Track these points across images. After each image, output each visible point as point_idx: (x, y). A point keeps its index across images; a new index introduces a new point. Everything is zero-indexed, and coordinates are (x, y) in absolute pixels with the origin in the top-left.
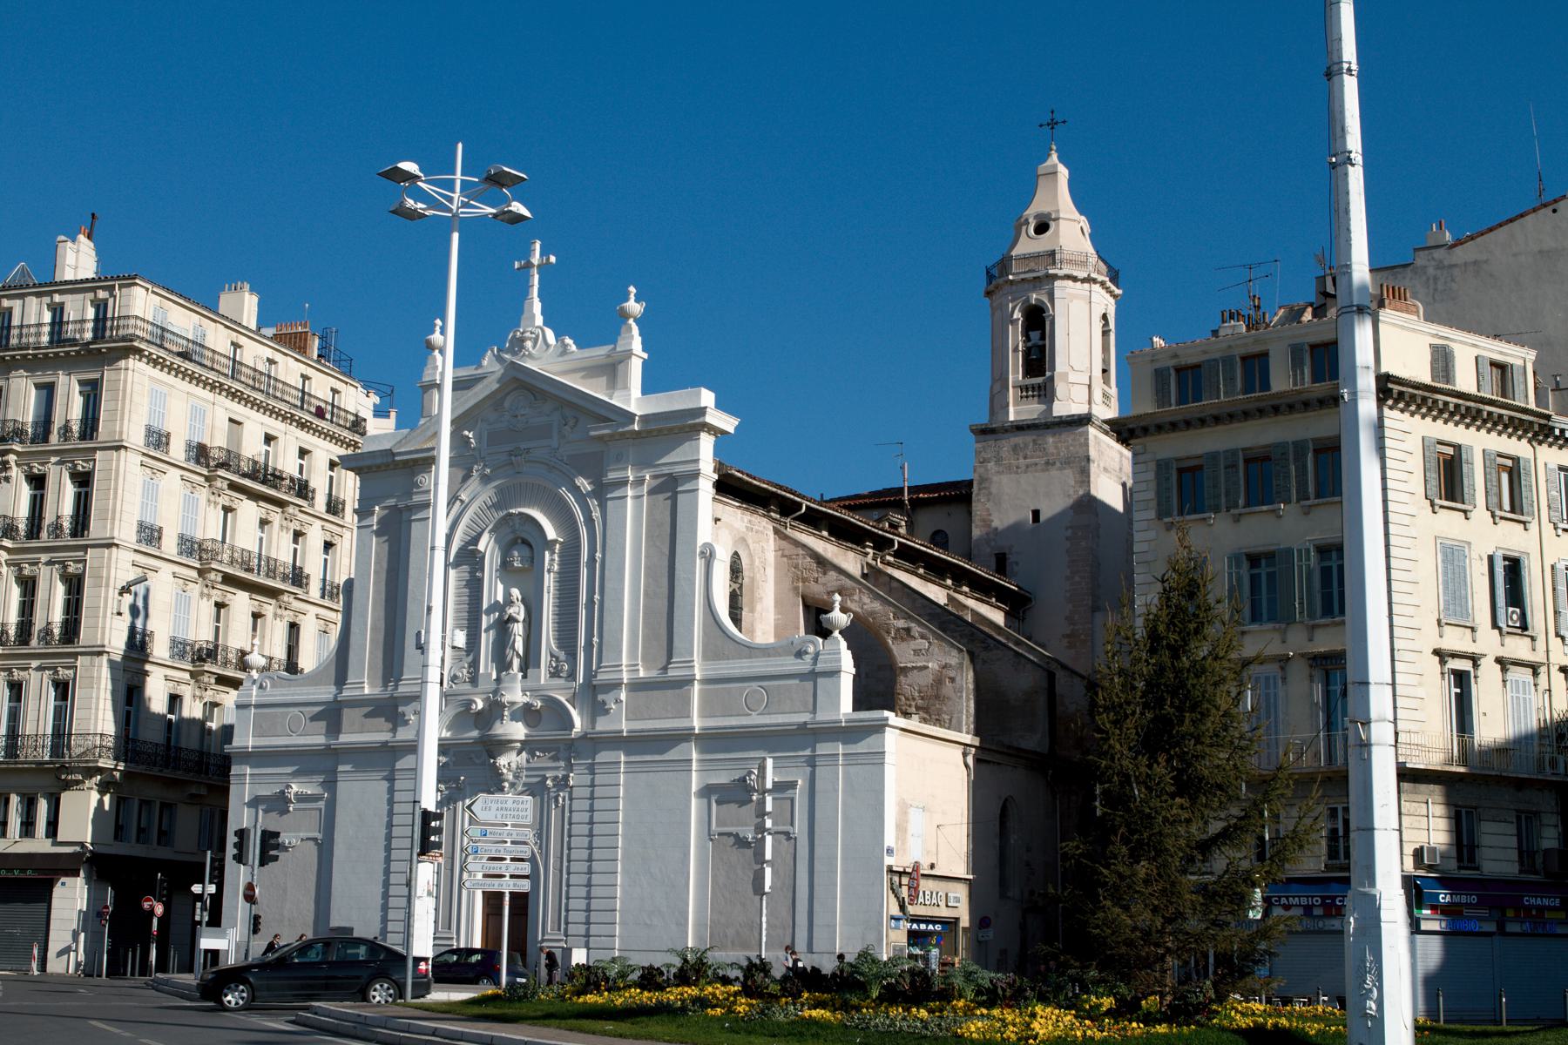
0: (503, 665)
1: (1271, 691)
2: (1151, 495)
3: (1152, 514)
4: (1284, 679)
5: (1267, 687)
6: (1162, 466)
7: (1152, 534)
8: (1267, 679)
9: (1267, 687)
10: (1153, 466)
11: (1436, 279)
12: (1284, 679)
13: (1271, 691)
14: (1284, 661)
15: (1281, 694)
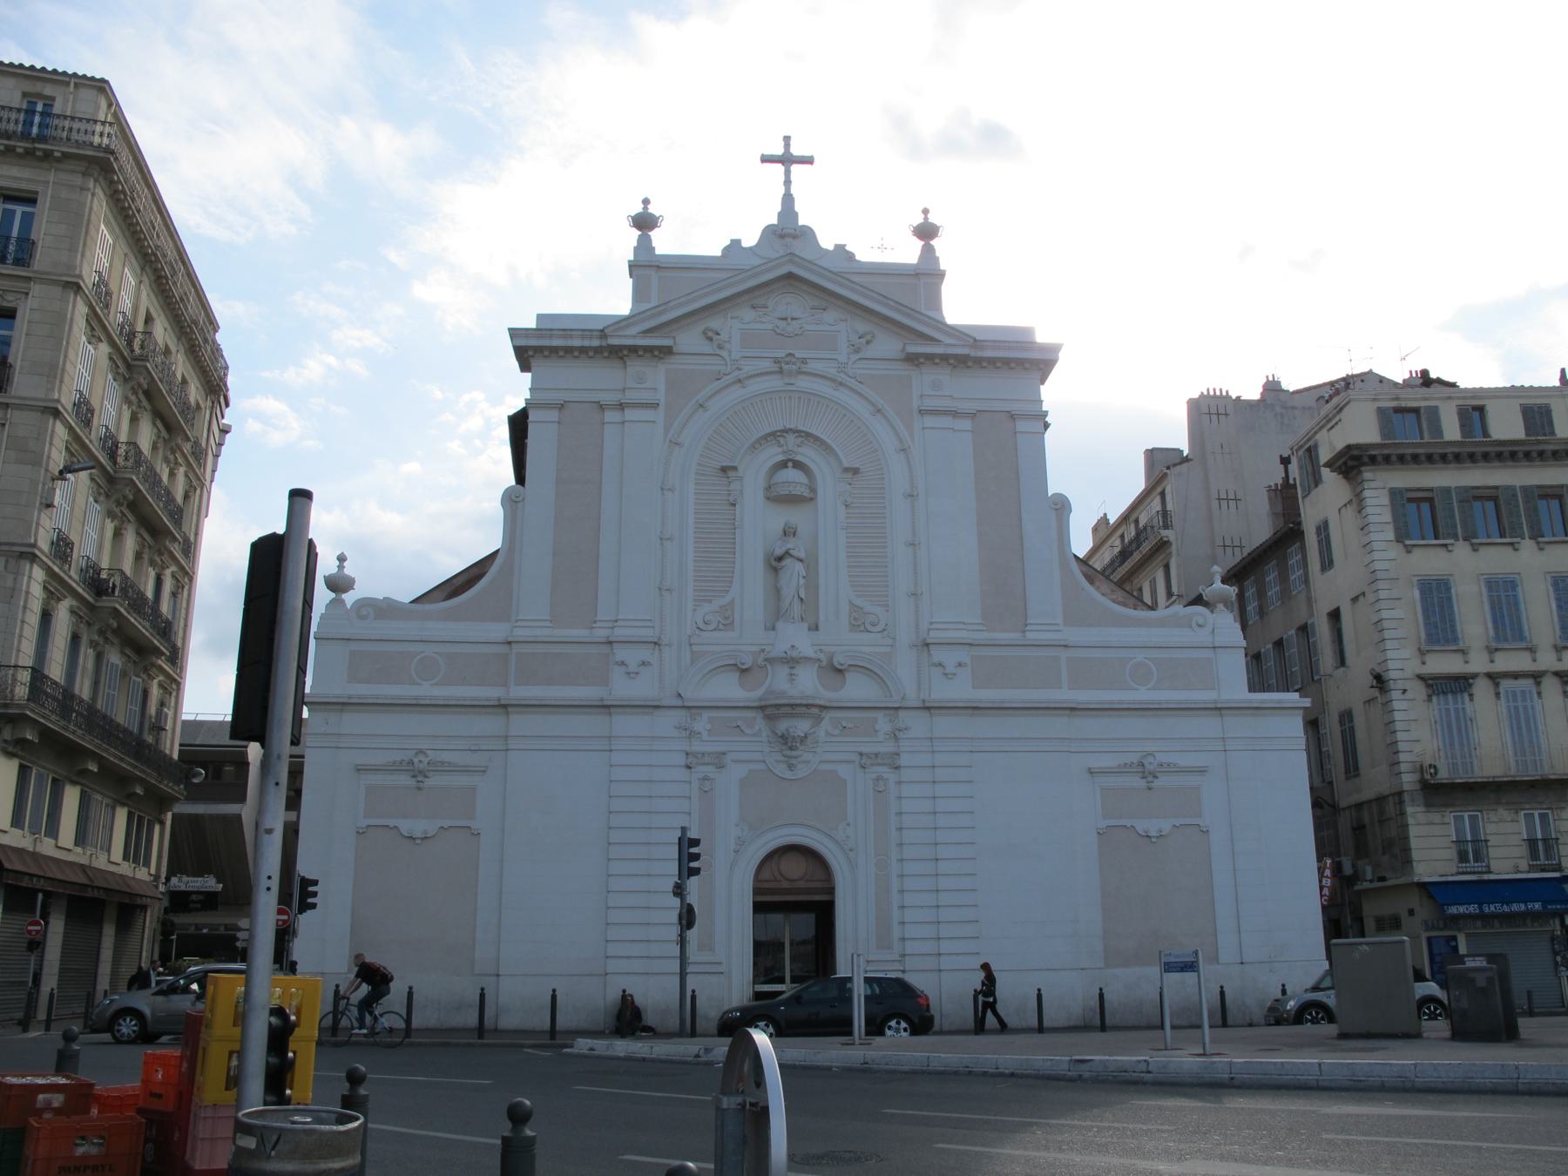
0: (776, 615)
1: (1529, 703)
2: (1388, 517)
3: (1391, 535)
4: (1539, 694)
5: (1524, 700)
6: (1395, 494)
7: (1392, 554)
8: (1523, 692)
9: (1524, 700)
10: (1386, 492)
11: (1282, 415)
12: (1539, 694)
13: (1529, 703)
14: (1537, 677)
15: (1538, 708)
